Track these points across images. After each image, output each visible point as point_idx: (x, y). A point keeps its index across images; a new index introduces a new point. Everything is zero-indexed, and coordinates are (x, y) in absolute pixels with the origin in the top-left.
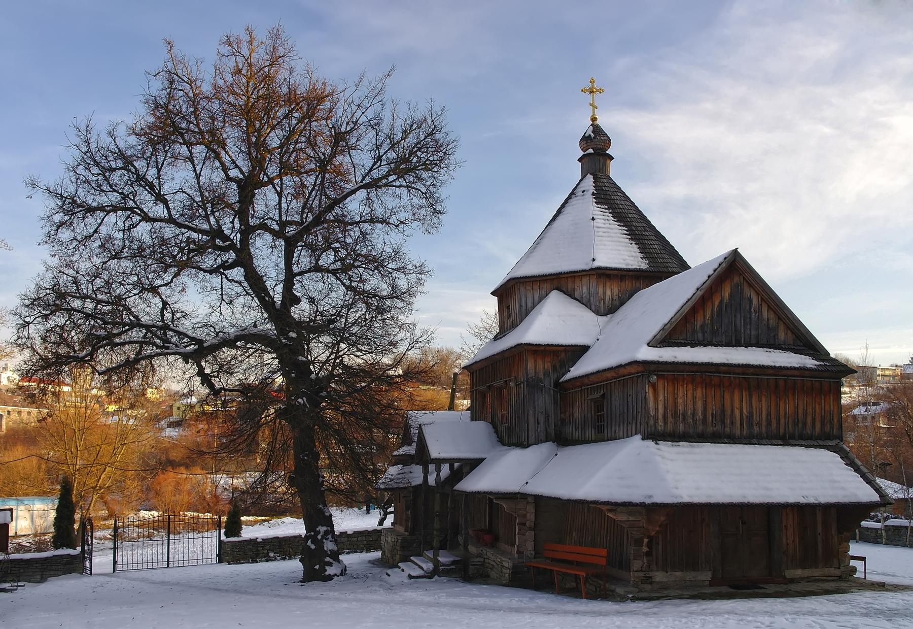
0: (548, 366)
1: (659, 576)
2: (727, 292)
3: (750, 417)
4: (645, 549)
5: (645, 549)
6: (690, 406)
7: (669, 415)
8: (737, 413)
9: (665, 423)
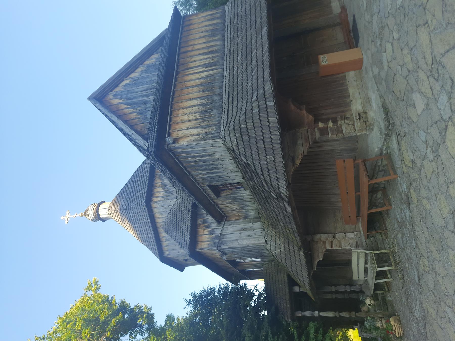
0: (206, 232)
1: (357, 106)
4: (331, 124)
5: (331, 124)
7: (203, 124)
8: (203, 74)
9: (210, 126)
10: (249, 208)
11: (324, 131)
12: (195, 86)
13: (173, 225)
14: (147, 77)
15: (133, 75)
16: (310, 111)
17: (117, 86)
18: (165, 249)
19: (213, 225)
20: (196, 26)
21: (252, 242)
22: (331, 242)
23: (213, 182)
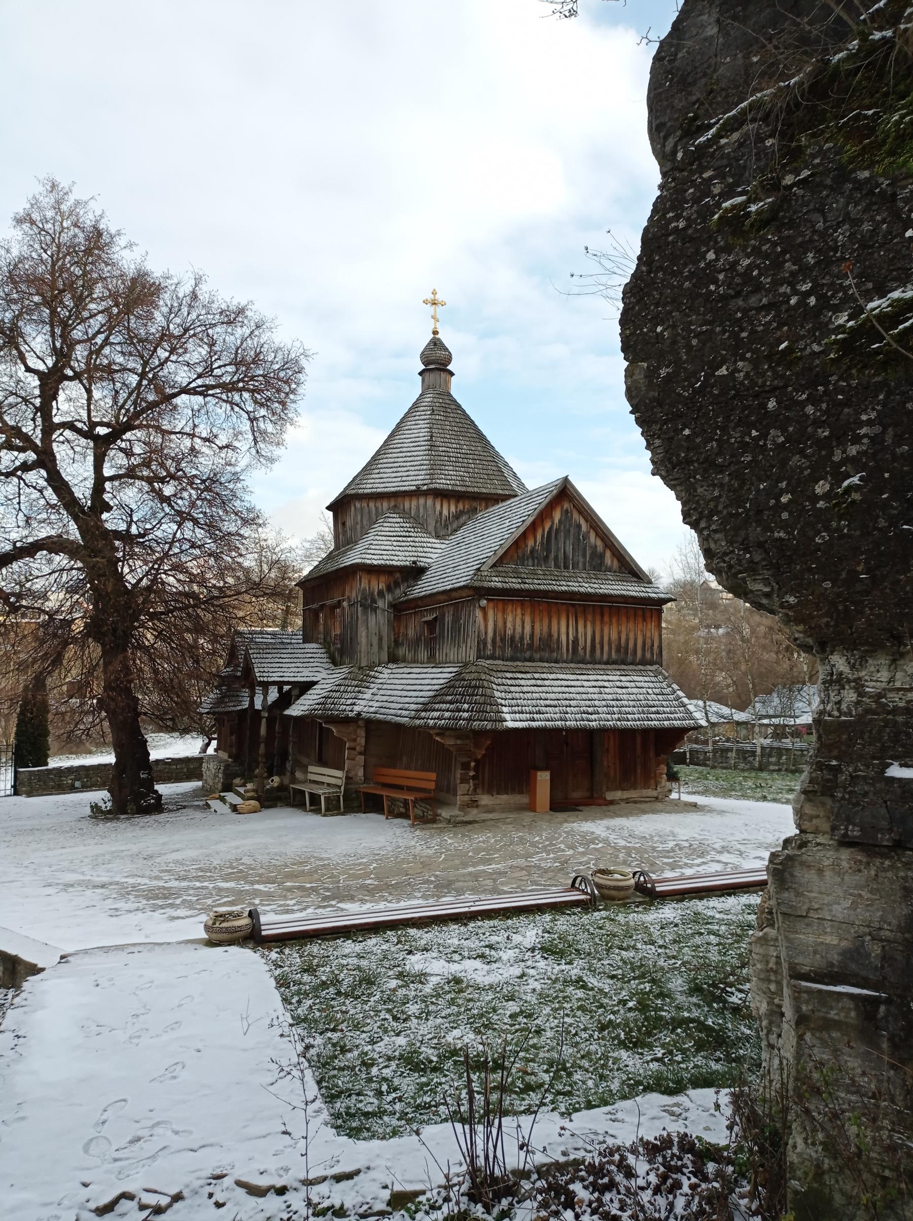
0: (382, 586)
1: (485, 800)
2: (557, 515)
3: (576, 641)
5: (472, 773)
6: (519, 629)
7: (498, 639)
8: (563, 638)
11: (465, 766)
12: (550, 629)
14: (584, 556)
15: (592, 535)
17: (580, 513)
20: (640, 626)
22: (354, 749)
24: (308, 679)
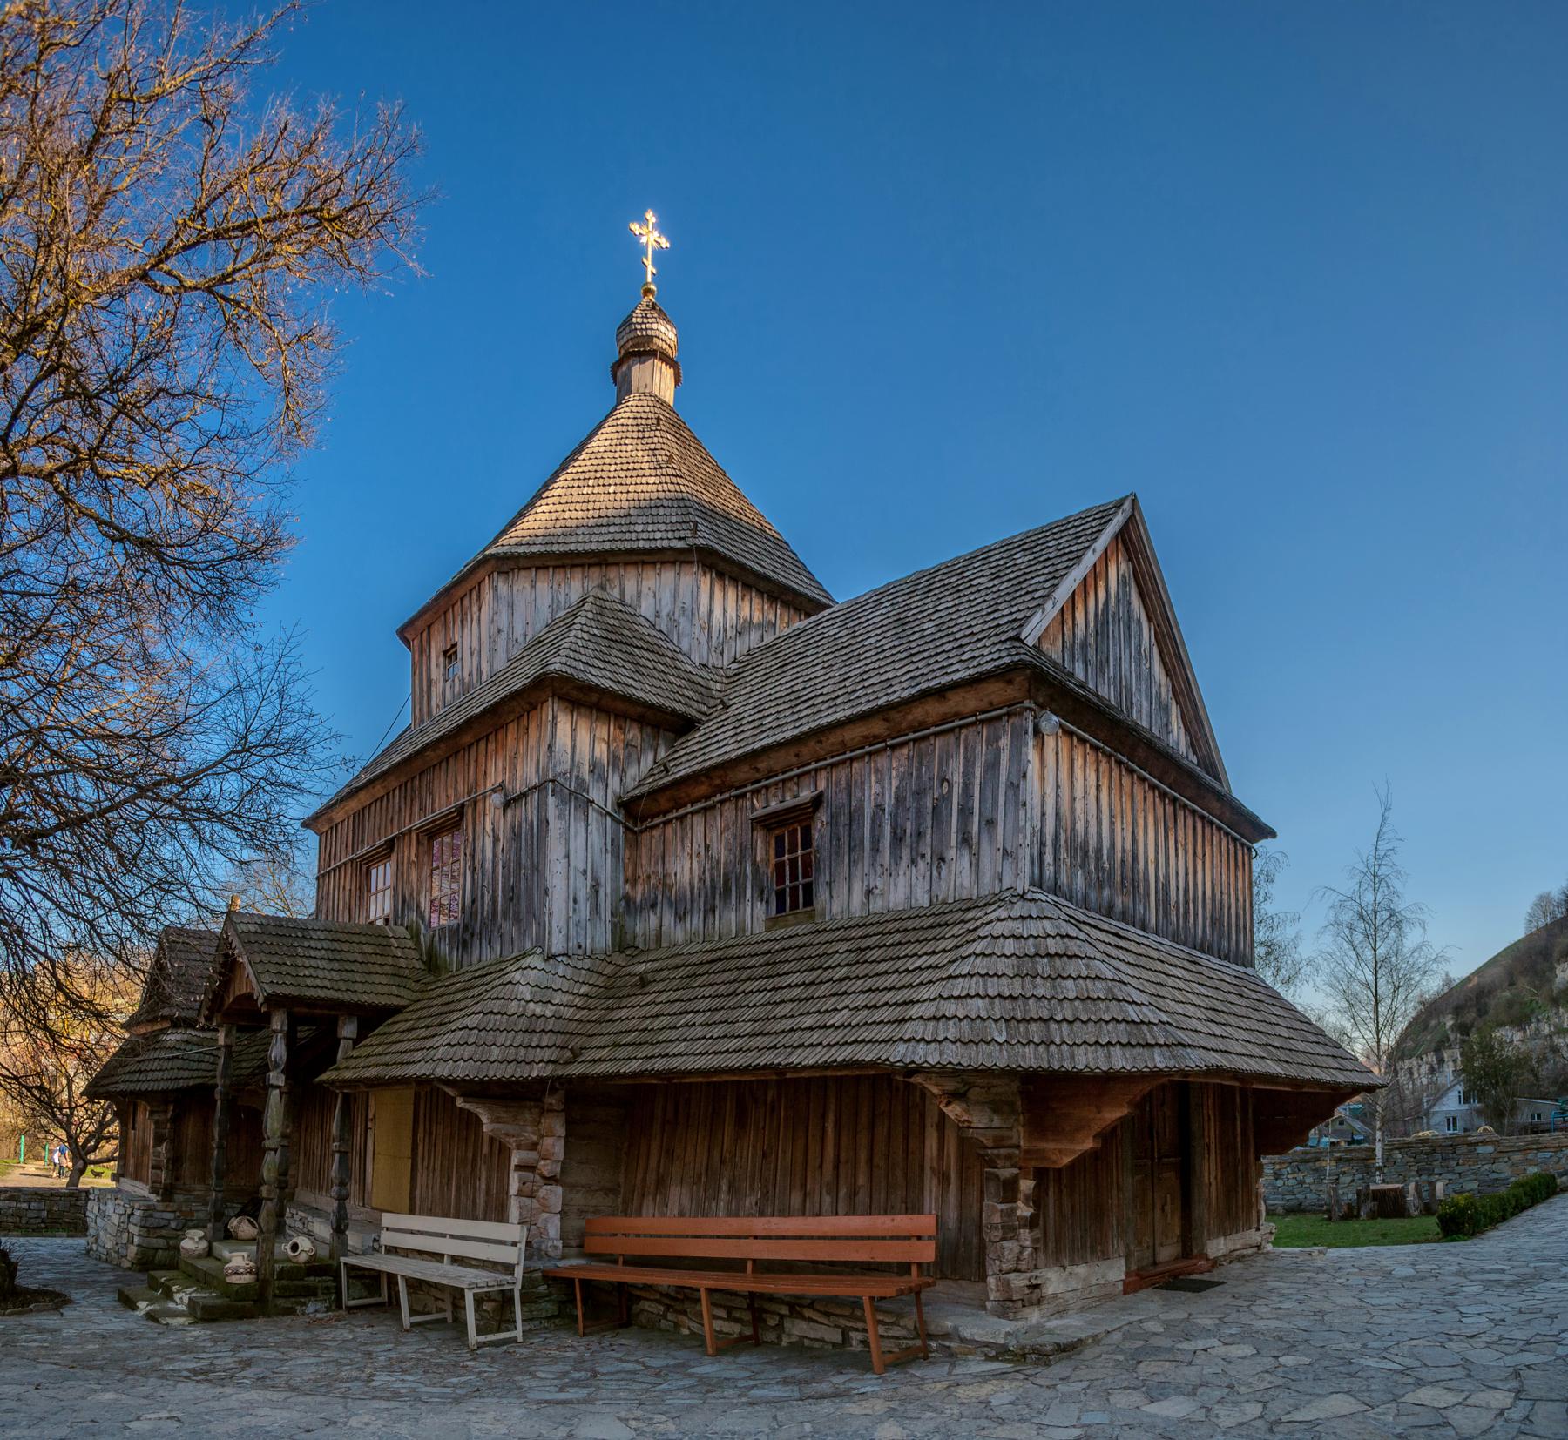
0: (601, 751)
4: (1024, 1210)
5: (1024, 1210)
10: (668, 919)
11: (1009, 1190)
13: (620, 632)
16: (1094, 1155)
18: (522, 582)
19: (617, 779)
21: (555, 909)
23: (833, 820)
24: (383, 1001)
